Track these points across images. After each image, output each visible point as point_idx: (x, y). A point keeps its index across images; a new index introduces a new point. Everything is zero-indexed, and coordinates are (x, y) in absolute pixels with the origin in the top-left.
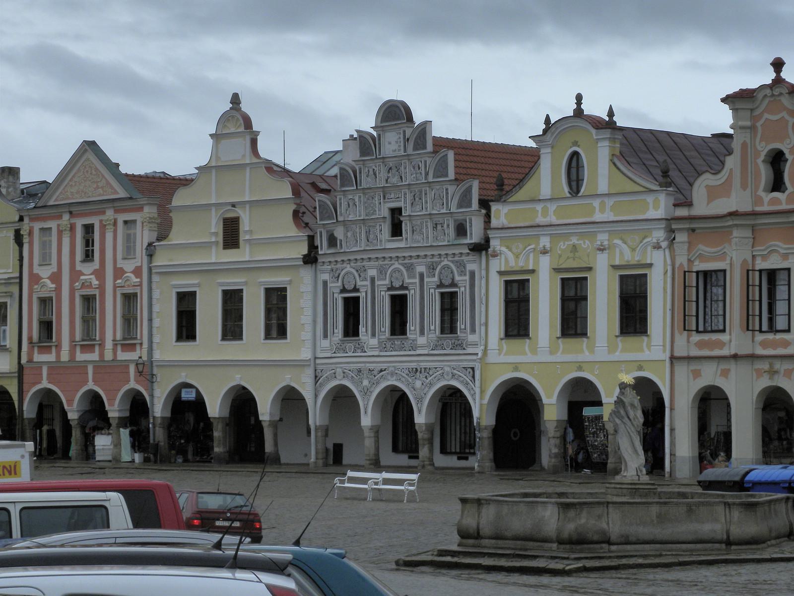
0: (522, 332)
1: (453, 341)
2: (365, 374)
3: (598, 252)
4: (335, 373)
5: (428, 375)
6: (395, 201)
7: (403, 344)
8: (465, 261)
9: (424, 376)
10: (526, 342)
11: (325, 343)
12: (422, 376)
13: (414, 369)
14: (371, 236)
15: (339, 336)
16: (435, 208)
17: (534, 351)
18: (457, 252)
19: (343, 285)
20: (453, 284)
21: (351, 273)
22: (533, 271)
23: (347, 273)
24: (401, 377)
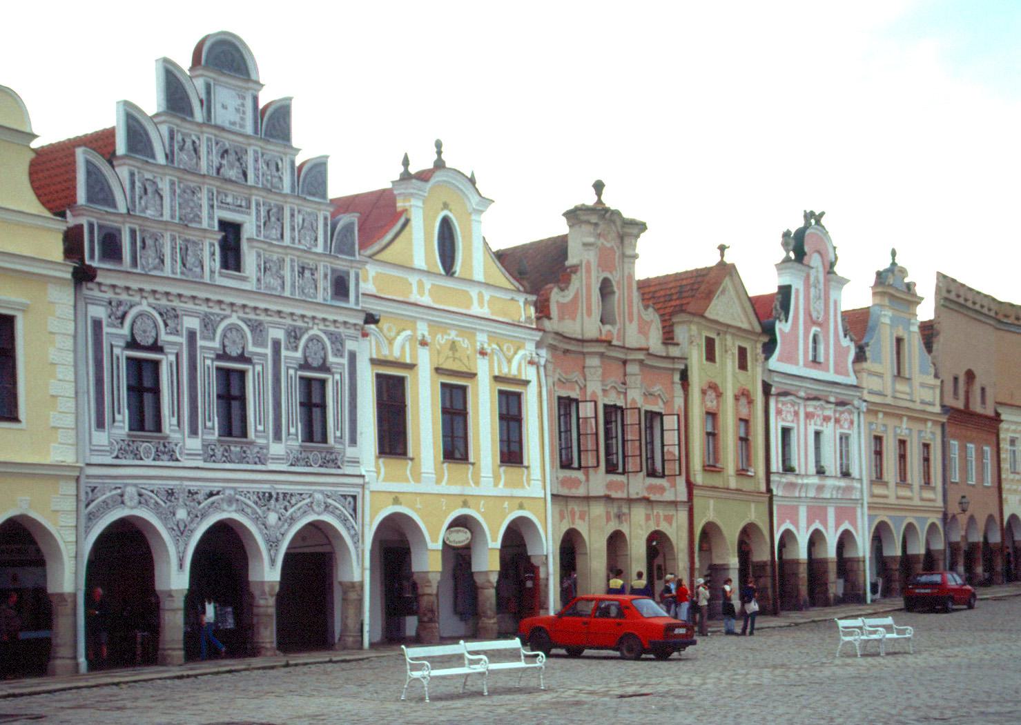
0: (399, 451)
1: (323, 455)
2: (181, 500)
3: (478, 356)
4: (122, 496)
5: (288, 504)
6: (234, 211)
7: (245, 452)
8: (343, 335)
9: (282, 507)
10: (407, 464)
11: (101, 438)
12: (280, 506)
13: (267, 495)
14: (191, 260)
15: (123, 428)
16: (303, 242)
17: (417, 477)
18: (341, 319)
19: (132, 335)
20: (324, 368)
21: (150, 317)
22: (411, 367)
23: (141, 315)
24: (244, 506)
